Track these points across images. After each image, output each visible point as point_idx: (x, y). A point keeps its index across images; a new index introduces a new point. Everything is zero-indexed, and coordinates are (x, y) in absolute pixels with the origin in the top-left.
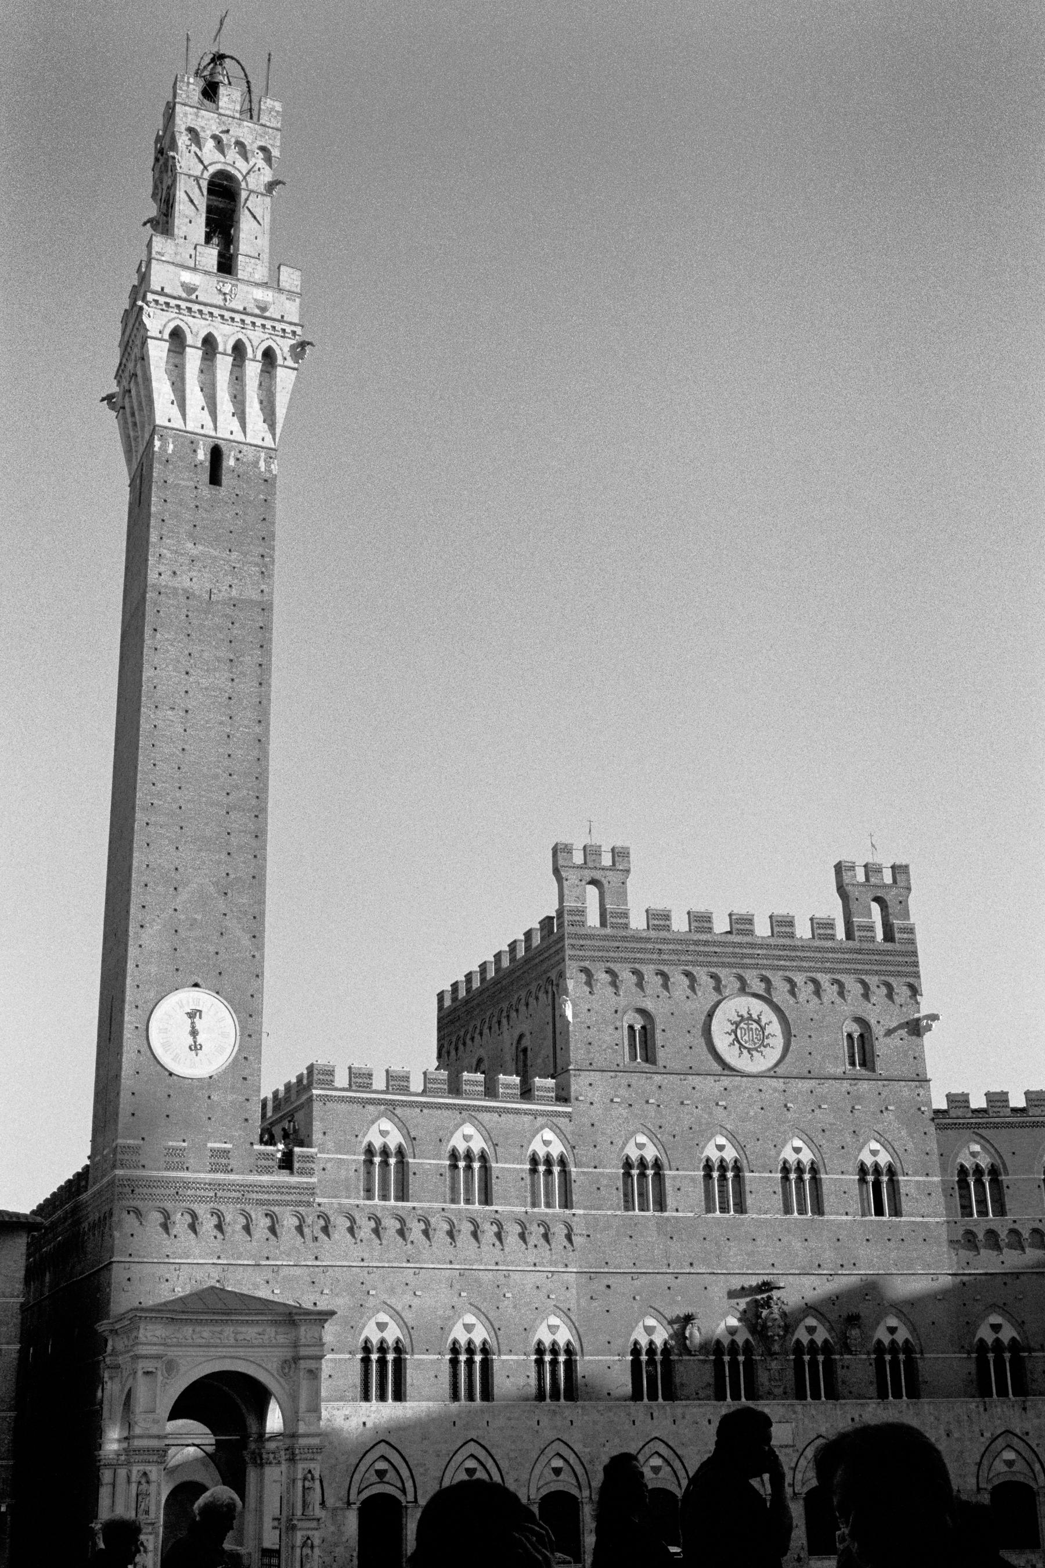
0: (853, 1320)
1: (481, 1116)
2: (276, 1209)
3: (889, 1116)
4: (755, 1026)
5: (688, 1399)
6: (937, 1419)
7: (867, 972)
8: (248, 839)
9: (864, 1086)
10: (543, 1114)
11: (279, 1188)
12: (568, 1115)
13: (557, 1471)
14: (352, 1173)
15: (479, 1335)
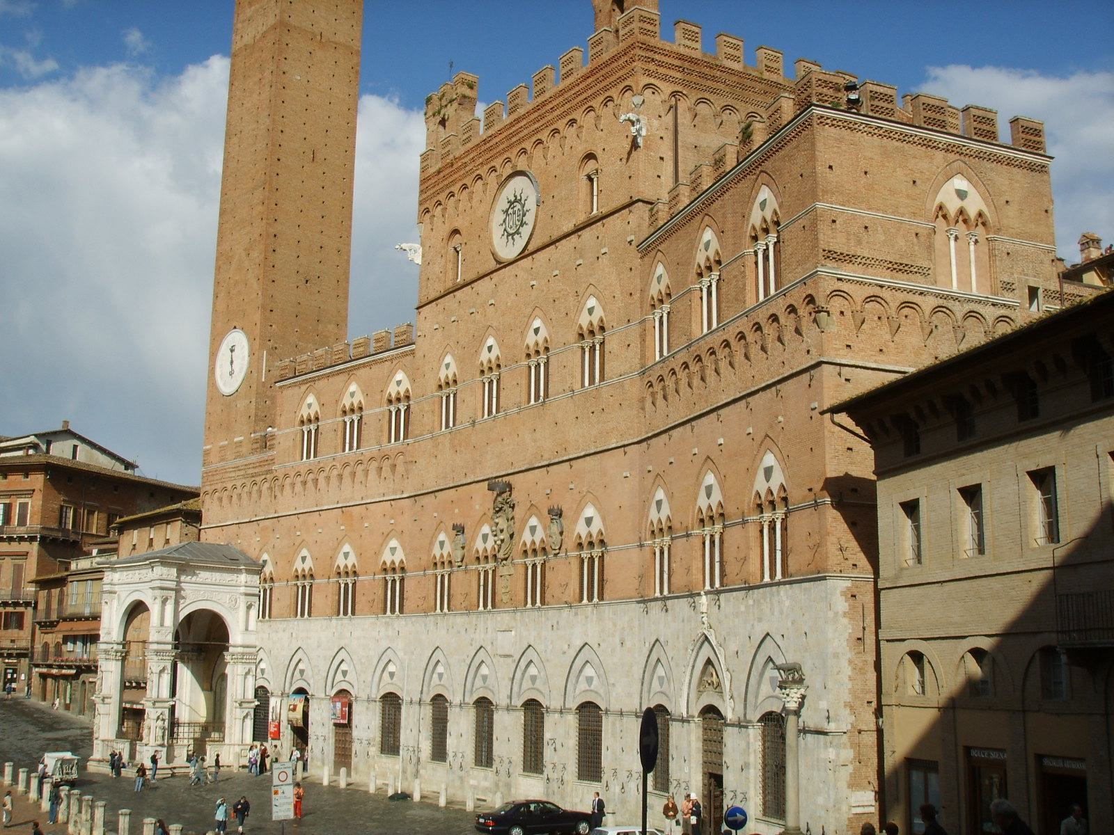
0: (557, 514)
1: (362, 372)
2: (258, 479)
3: (604, 260)
4: (518, 206)
5: (456, 609)
6: (615, 625)
7: (594, 96)
8: (260, 208)
9: (586, 234)
10: (397, 357)
11: (261, 463)
12: (413, 352)
13: (392, 675)
14: (291, 443)
15: (352, 560)
